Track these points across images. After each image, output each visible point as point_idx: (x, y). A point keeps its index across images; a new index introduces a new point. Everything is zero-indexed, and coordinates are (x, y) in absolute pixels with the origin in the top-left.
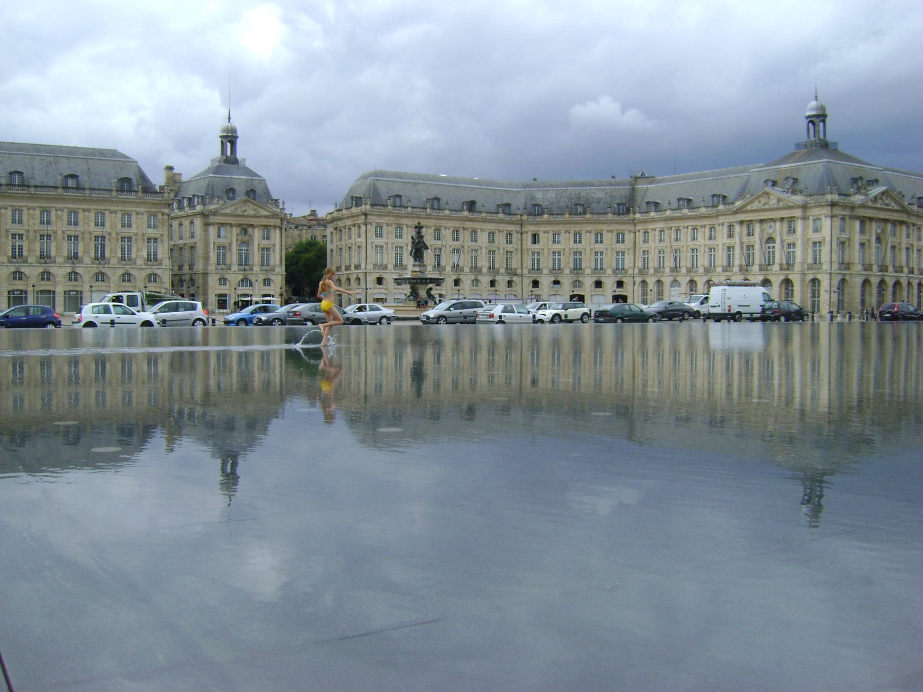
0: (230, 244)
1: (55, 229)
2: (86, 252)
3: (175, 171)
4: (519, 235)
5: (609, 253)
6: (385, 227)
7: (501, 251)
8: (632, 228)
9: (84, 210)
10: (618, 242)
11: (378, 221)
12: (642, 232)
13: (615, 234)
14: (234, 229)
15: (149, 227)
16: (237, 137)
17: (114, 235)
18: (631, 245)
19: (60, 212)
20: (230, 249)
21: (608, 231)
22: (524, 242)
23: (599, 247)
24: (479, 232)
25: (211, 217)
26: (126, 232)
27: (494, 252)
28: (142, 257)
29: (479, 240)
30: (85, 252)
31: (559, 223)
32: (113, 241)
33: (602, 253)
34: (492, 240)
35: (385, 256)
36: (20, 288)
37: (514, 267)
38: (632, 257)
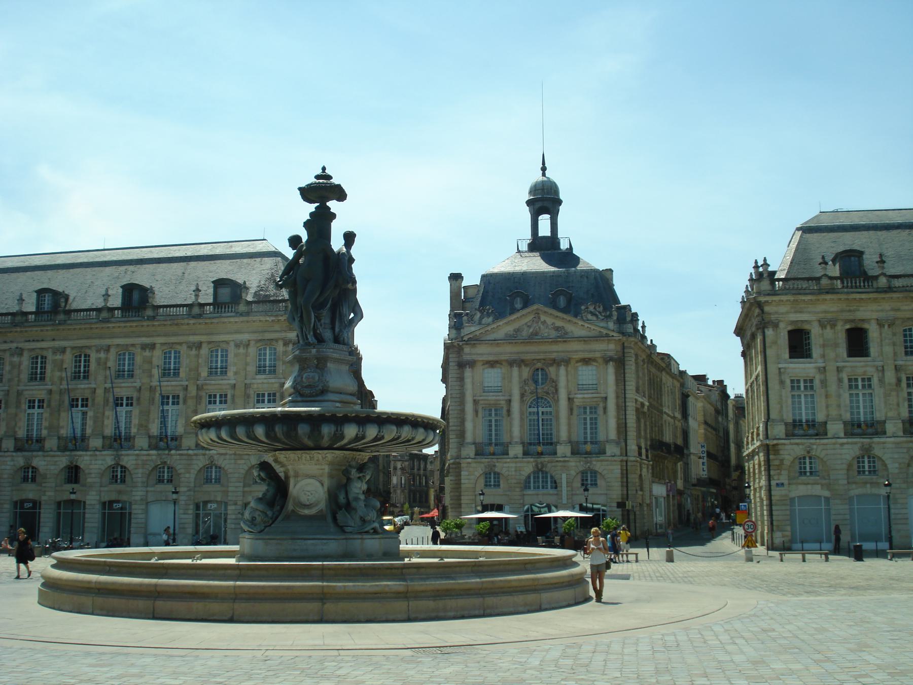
1: (93, 386)
2: (143, 426)
3: (465, 283)
9: (144, 347)
11: (794, 317)
14: (515, 370)
15: (261, 370)
16: (559, 202)
17: (193, 391)
19: (102, 355)
20: (509, 411)
25: (467, 349)
30: (140, 426)
32: (191, 403)
35: (820, 402)
36: (31, 496)
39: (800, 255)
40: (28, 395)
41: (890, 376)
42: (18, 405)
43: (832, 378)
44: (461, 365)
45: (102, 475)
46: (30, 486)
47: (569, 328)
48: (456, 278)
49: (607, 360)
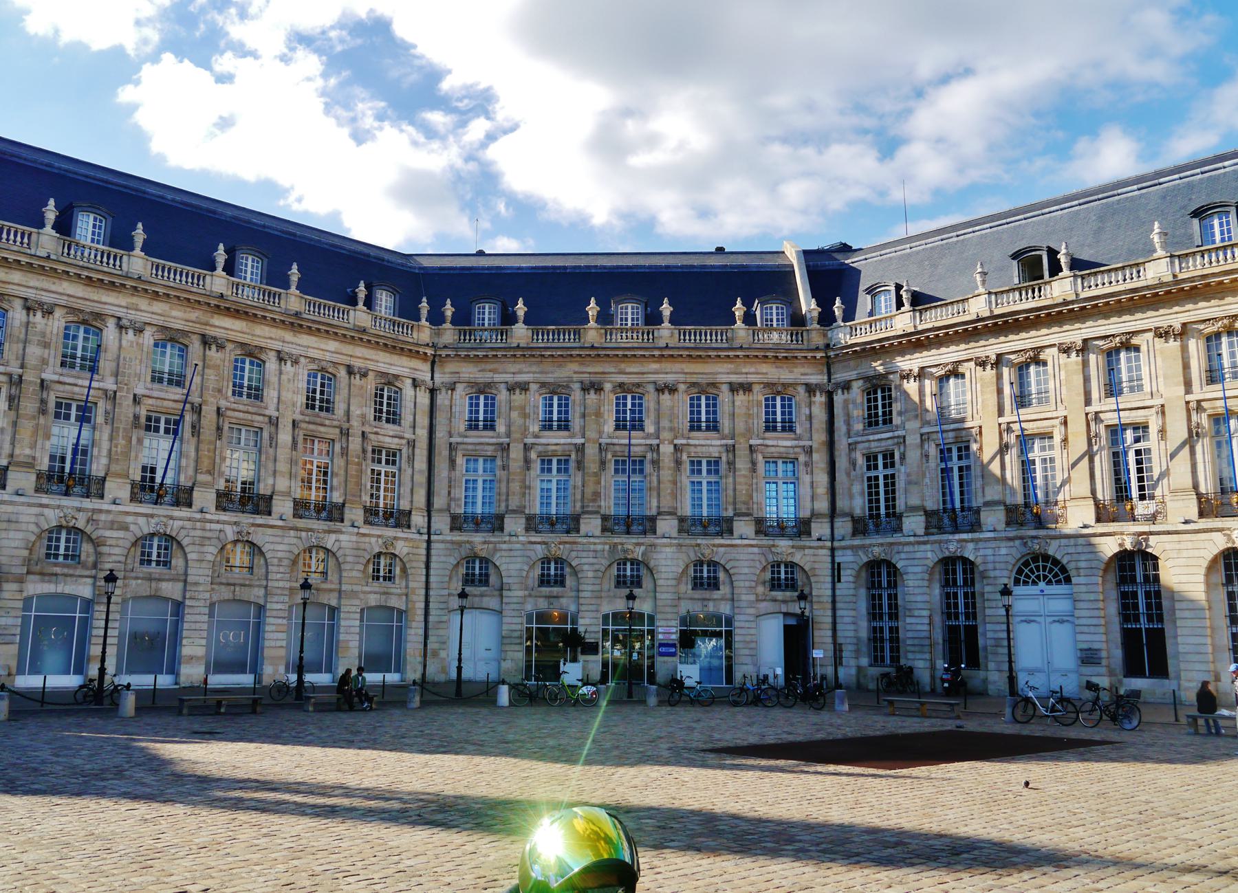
4: (424, 399)
5: (742, 465)
7: (355, 444)
8: (817, 377)
10: (770, 426)
12: (857, 386)
13: (759, 395)
18: (820, 437)
21: (734, 388)
22: (441, 419)
23: (708, 444)
31: (567, 356)
33: (714, 464)
34: (318, 401)
37: (404, 505)
38: (822, 479)
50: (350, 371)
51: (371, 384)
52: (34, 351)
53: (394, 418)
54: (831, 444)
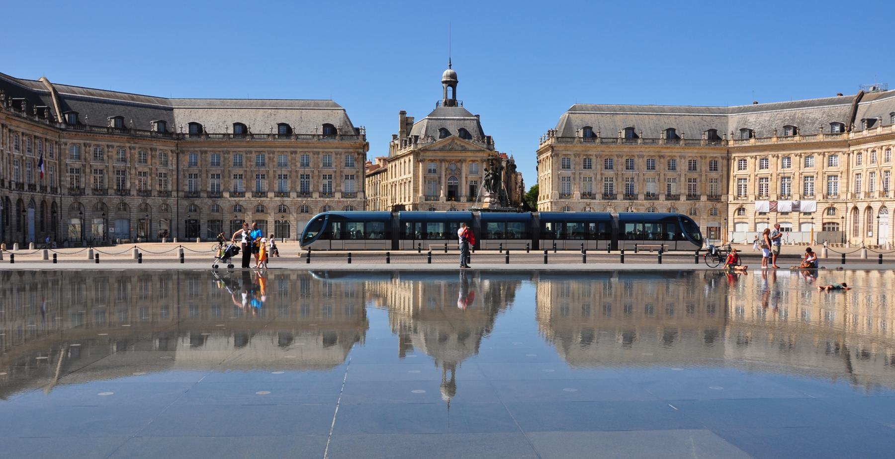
0: (440, 178)
2: (293, 189)
3: (407, 116)
4: (725, 162)
6: (572, 158)
7: (703, 178)
9: (292, 153)
11: (565, 152)
15: (347, 165)
17: (316, 173)
20: (440, 182)
21: (819, 154)
24: (678, 160)
26: (327, 171)
27: (695, 180)
28: (340, 191)
29: (678, 168)
34: (693, 167)
38: (845, 181)
39: (568, 125)
40: (234, 172)
41: (599, 177)
42: (230, 177)
43: (577, 176)
44: (417, 161)
45: (274, 209)
46: (238, 214)
47: (467, 146)
48: (403, 113)
49: (483, 161)
50: (701, 157)
51: (708, 160)
52: (620, 167)
53: (716, 169)
54: (848, 170)
